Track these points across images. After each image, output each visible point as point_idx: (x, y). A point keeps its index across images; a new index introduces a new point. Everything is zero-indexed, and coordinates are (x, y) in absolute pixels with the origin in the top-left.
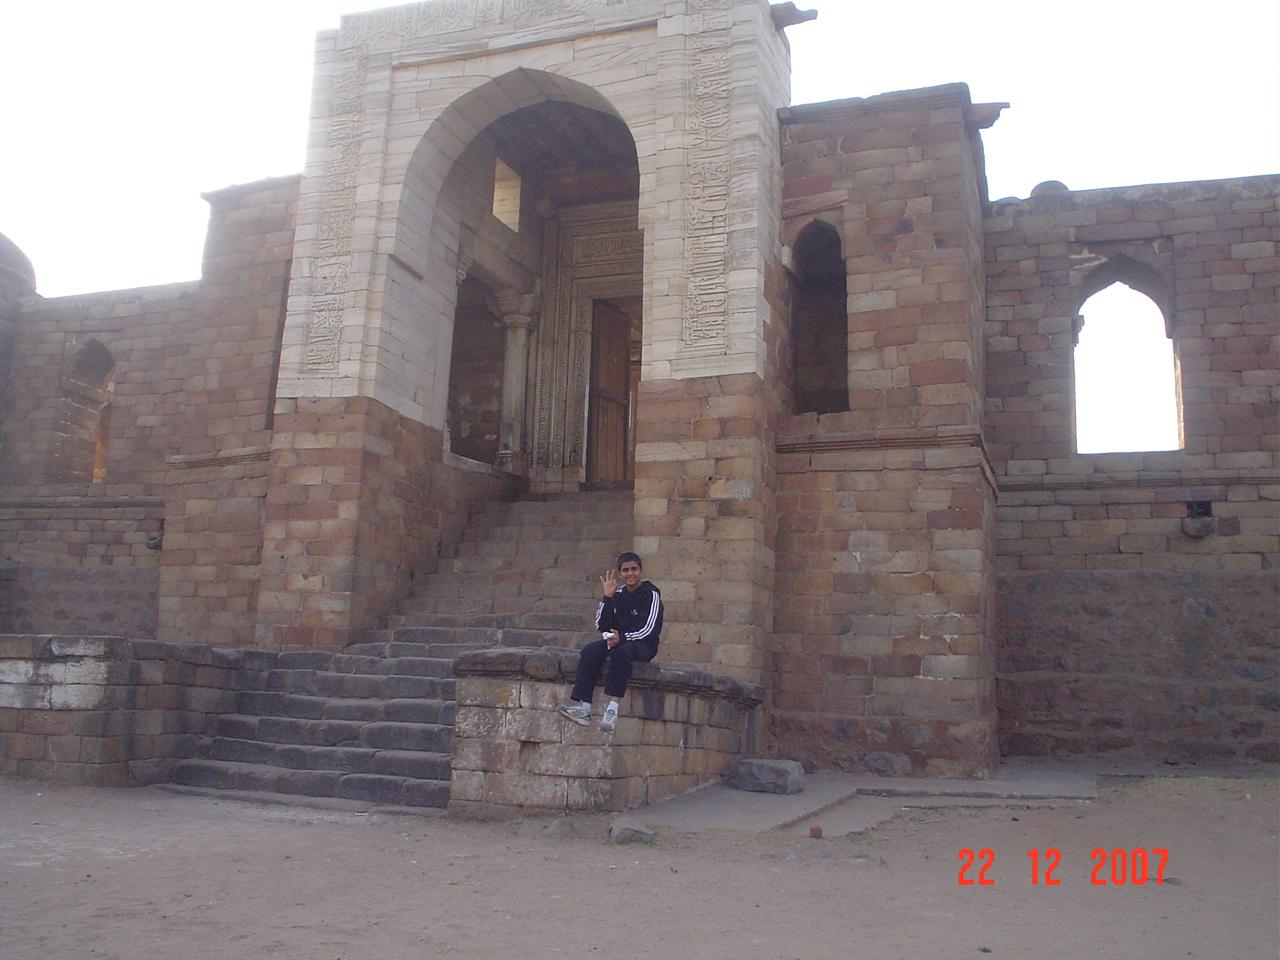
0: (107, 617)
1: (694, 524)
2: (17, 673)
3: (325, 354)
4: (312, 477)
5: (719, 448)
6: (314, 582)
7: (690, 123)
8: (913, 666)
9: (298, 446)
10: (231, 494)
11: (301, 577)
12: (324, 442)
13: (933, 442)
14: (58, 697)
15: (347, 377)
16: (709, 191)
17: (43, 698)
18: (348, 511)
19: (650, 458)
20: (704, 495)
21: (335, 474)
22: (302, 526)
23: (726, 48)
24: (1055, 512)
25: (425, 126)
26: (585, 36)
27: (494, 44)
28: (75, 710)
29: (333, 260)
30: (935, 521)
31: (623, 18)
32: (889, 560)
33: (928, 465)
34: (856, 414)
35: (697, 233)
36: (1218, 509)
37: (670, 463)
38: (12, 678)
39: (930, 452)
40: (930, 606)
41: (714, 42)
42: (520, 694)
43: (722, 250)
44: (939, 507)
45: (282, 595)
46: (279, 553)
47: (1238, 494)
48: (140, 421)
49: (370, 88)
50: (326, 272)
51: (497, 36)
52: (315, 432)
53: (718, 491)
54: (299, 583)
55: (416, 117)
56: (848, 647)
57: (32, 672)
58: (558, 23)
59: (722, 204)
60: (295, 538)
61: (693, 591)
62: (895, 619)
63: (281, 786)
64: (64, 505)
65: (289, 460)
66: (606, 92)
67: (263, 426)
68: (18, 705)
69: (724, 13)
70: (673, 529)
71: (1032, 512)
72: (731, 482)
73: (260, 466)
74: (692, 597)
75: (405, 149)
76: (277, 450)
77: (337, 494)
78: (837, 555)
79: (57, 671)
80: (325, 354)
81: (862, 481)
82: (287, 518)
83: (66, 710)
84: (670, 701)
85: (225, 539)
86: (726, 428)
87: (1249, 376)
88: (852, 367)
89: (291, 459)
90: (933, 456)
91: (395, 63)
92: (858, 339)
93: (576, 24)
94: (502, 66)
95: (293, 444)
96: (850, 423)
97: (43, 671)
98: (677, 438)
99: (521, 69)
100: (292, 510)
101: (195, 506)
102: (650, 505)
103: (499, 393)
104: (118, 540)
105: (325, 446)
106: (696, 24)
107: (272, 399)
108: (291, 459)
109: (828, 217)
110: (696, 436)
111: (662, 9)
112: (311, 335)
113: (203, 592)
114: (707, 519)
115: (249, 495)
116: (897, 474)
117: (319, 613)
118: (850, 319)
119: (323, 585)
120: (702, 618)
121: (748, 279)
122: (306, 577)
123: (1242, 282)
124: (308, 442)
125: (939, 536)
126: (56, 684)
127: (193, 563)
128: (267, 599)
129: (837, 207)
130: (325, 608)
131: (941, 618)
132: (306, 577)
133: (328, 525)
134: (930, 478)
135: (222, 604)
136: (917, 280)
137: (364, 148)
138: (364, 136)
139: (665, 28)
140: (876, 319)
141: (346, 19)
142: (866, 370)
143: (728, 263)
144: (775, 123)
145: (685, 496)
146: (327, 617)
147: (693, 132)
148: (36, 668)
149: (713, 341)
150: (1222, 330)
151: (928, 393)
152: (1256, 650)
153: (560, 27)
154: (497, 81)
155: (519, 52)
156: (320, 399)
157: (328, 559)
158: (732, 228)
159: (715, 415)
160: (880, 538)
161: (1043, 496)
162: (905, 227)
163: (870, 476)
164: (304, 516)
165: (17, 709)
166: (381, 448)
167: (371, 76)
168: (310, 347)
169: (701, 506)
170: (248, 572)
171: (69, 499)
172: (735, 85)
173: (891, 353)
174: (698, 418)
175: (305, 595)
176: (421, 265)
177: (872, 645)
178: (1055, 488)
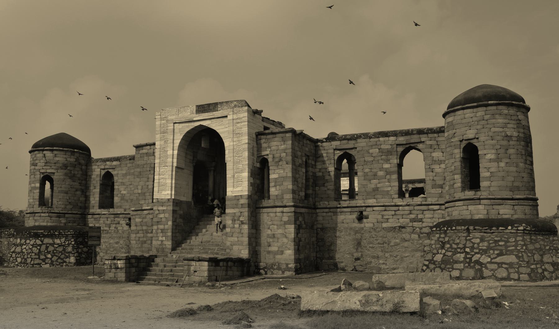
0: (117, 243)
1: (237, 226)
4: (162, 216)
8: (282, 253)
10: (145, 218)
12: (164, 208)
13: (285, 206)
18: (170, 223)
20: (238, 220)
21: (167, 215)
22: (161, 227)
23: (241, 122)
24: (330, 214)
25: (181, 137)
27: (195, 119)
30: (285, 223)
36: (364, 213)
39: (285, 209)
40: (285, 240)
41: (239, 121)
42: (193, 263)
47: (368, 209)
48: (122, 192)
50: (162, 170)
53: (241, 219)
54: (160, 238)
56: (270, 249)
64: (104, 214)
66: (218, 131)
71: (325, 214)
73: (151, 211)
75: (177, 142)
81: (272, 215)
84: (221, 264)
87: (373, 181)
90: (285, 210)
92: (272, 184)
96: (270, 203)
103: (208, 186)
104: (119, 223)
106: (235, 117)
107: (153, 199)
109: (265, 157)
120: (239, 245)
121: (246, 174)
123: (371, 159)
125: (287, 226)
128: (154, 242)
129: (268, 155)
133: (166, 227)
134: (284, 214)
135: (145, 242)
136: (282, 172)
142: (273, 191)
143: (242, 171)
144: (254, 136)
150: (367, 170)
152: (371, 245)
154: (196, 127)
159: (240, 203)
161: (327, 210)
163: (274, 214)
166: (177, 208)
167: (169, 125)
170: (149, 235)
171: (105, 213)
175: (162, 241)
176: (183, 166)
177: (274, 248)
178: (330, 208)
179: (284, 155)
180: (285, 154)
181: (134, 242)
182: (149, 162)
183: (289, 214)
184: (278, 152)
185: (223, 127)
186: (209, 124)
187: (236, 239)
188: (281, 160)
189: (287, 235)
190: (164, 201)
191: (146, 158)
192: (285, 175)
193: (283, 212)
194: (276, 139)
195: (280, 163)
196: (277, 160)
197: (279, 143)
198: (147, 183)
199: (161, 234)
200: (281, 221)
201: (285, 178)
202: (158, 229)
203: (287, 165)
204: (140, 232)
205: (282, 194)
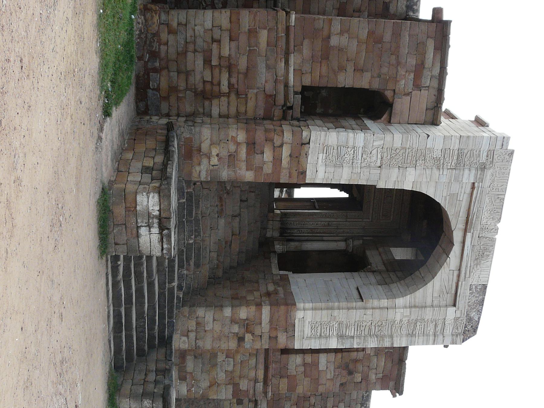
1: (236, 329)
2: (154, 205)
3: (331, 156)
4: (268, 156)
5: (266, 337)
6: (215, 160)
7: (405, 320)
8: (182, 378)
9: (285, 145)
10: (268, 67)
11: (218, 152)
14: (143, 231)
15: (317, 171)
16: (373, 327)
17: (142, 222)
19: (263, 312)
20: (248, 331)
21: (268, 169)
22: (243, 152)
26: (459, 276)
27: (469, 235)
28: (138, 240)
29: (379, 156)
30: (236, 386)
31: (461, 293)
32: (222, 371)
33: (257, 384)
34: (279, 357)
35: (356, 324)
37: (261, 319)
38: (151, 203)
40: (205, 384)
41: (439, 328)
43: (347, 334)
44: (241, 387)
45: (208, 142)
46: (230, 138)
49: (467, 171)
50: (374, 152)
51: (473, 237)
52: (290, 156)
53: (248, 337)
54: (214, 151)
55: (445, 194)
57: (154, 214)
58: (469, 265)
59: (366, 333)
60: (237, 148)
61: (209, 329)
62: (200, 373)
63: (115, 284)
65: (277, 141)
66: (430, 285)
67: (304, 84)
68: (138, 208)
69: (451, 332)
70: (233, 321)
72: (251, 341)
74: (206, 329)
76: (283, 135)
77: (259, 169)
78: (225, 354)
79: (155, 230)
80: (331, 156)
81: (253, 362)
82: (248, 144)
83: (138, 236)
85: (243, 63)
86: (273, 339)
88: (297, 356)
89: (277, 143)
90: (260, 386)
91: (476, 185)
93: (465, 273)
94: (457, 236)
95: (286, 143)
97: (156, 221)
98: (271, 322)
99: (453, 244)
100: (251, 145)
101: (263, 36)
102: (243, 313)
105: (283, 162)
108: (277, 143)
110: (271, 328)
111: (460, 309)
112: (342, 147)
113: (215, 45)
114: (237, 333)
115: (266, 82)
116: (254, 373)
117: (199, 164)
118: (317, 355)
119: (213, 166)
122: (217, 155)
124: (286, 152)
125: (230, 388)
126: (150, 229)
127: (231, 39)
130: (202, 167)
131: (200, 387)
132: (217, 155)
133: (243, 165)
134: (252, 383)
135: (207, 61)
137: (435, 171)
138: (441, 171)
139: (451, 311)
140: (316, 364)
141: (512, 153)
143: (341, 337)
145: (248, 326)
146: (198, 168)
147: (401, 321)
148: (155, 217)
149: (310, 331)
150: (313, 400)
151: (285, 380)
153: (467, 266)
155: (462, 245)
156: (307, 157)
157: (226, 167)
158: (355, 339)
159: (279, 335)
160: (230, 368)
162: (350, 373)
164: (248, 154)
165: (136, 207)
167: (473, 172)
168: (336, 148)
169: (243, 330)
172: (417, 338)
173: (302, 369)
174: (278, 329)
179: (358, 377)
180: (359, 380)
181: (208, 24)
182: (402, 72)
183: (251, 392)
184: (366, 369)
185: (436, 295)
186: (449, 266)
187: (209, 327)
188: (350, 373)
189: (215, 388)
190: (302, 159)
191: (412, 61)
192: (323, 381)
193: (256, 381)
194: (389, 365)
195: (345, 372)
196: (351, 366)
197: (381, 369)
198: (350, 68)
199: (224, 153)
200: (240, 377)
201: (316, 381)
202: (238, 144)
203: (338, 384)
204: (233, 44)
205: (288, 377)
